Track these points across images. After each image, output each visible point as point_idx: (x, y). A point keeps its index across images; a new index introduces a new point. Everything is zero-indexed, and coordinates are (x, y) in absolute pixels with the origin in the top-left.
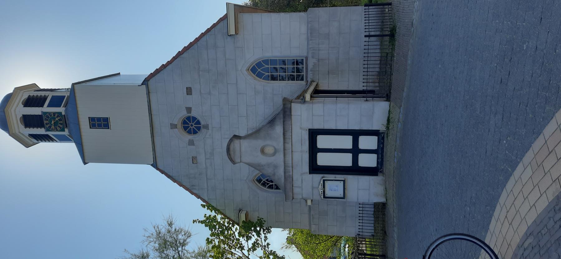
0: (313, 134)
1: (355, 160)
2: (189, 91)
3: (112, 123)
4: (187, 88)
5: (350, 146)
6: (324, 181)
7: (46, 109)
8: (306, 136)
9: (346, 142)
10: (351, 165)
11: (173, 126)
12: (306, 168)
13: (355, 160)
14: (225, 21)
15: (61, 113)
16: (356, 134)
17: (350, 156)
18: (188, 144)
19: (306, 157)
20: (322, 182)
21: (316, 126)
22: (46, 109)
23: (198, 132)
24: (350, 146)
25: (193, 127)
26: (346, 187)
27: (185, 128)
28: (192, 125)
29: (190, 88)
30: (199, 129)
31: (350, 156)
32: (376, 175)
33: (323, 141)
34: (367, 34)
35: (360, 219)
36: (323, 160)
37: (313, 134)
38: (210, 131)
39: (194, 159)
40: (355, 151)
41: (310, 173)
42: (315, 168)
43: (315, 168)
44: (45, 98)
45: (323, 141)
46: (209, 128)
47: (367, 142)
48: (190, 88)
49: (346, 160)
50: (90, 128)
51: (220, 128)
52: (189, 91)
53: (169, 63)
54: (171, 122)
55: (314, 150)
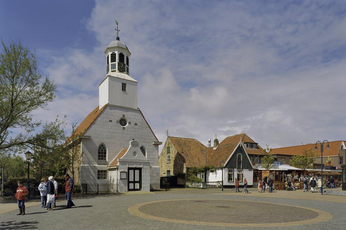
0: (140, 169)
2: (136, 124)
5: (136, 180)
6: (126, 172)
7: (126, 65)
9: (137, 179)
11: (124, 116)
12: (130, 166)
16: (140, 182)
17: (133, 180)
22: (126, 65)
24: (136, 180)
27: (122, 119)
31: (133, 180)
32: (128, 189)
33: (137, 172)
36: (131, 172)
37: (140, 169)
38: (122, 129)
39: (111, 121)
40: (134, 182)
41: (128, 168)
42: (129, 169)
43: (129, 169)
44: (128, 65)
49: (131, 179)
52: (136, 124)
53: (145, 119)
55: (134, 169)
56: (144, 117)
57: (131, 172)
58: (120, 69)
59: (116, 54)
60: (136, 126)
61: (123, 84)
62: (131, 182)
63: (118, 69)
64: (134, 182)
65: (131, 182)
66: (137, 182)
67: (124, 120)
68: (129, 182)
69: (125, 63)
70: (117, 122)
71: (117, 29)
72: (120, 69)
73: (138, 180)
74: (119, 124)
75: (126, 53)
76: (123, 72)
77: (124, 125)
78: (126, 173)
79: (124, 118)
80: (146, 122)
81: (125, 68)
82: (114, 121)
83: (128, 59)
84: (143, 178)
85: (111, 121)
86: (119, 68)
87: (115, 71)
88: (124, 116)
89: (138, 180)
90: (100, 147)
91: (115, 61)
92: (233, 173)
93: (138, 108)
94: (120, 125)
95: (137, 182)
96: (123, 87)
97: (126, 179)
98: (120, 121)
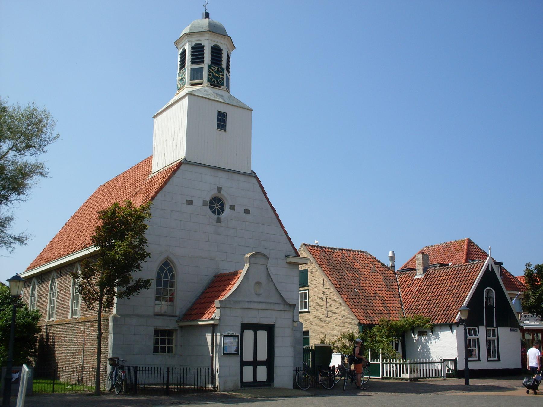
0: (270, 329)
2: (247, 212)
4: (250, 210)
5: (259, 359)
6: (238, 336)
9: (262, 356)
11: (219, 189)
12: (246, 321)
14: (294, 254)
16: (270, 363)
17: (251, 359)
18: (204, 199)
19: (255, 321)
20: (237, 334)
23: (211, 211)
24: (259, 359)
25: (216, 207)
26: (231, 355)
27: (214, 199)
28: (217, 206)
29: (250, 213)
30: (214, 212)
31: (251, 359)
33: (262, 335)
34: (170, 369)
35: (146, 368)
37: (270, 329)
38: (215, 223)
39: (189, 202)
40: (255, 363)
42: (245, 327)
46: (217, 223)
47: (262, 372)
48: (250, 213)
49: (248, 356)
50: (226, 113)
51: (218, 234)
52: (247, 212)
53: (268, 199)
54: (223, 188)
55: (255, 328)
56: (265, 194)
57: (249, 335)
58: (213, 80)
59: (203, 47)
60: (248, 217)
61: (219, 113)
62: (248, 363)
63: (209, 80)
64: (255, 363)
65: (248, 363)
66: (262, 363)
67: (220, 200)
68: (243, 363)
69: (224, 66)
70: (205, 203)
72: (213, 80)
74: (208, 207)
75: (226, 45)
76: (219, 87)
77: (219, 213)
78: (237, 338)
79: (219, 195)
80: (271, 205)
81: (223, 79)
82: (197, 203)
83: (228, 58)
84: (278, 351)
85: (189, 202)
86: (210, 77)
87: (201, 84)
88: (219, 189)
90: (161, 269)
91: (202, 62)
92: (496, 337)
94: (210, 212)
95: (262, 363)
96: (219, 120)
97: (238, 354)
98: (211, 202)
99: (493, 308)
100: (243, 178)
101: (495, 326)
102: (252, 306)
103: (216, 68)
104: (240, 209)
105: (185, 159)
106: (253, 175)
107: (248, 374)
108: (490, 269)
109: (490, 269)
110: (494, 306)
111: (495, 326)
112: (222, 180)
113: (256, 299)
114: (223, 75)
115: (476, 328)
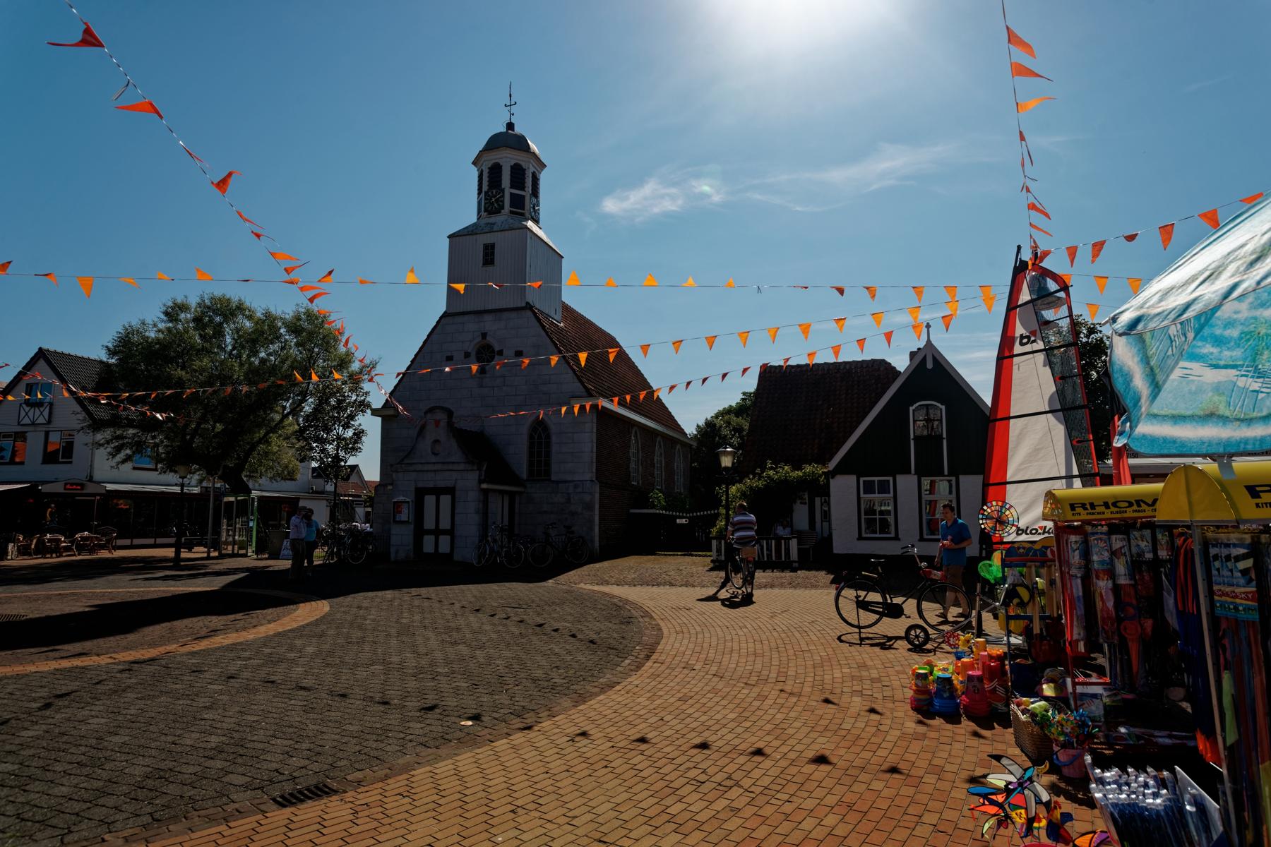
1: (429, 532)
3: (490, 268)
8: (449, 484)
9: (445, 524)
10: (425, 528)
11: (484, 335)
12: (420, 485)
13: (429, 532)
14: (585, 394)
15: (503, 209)
16: (451, 532)
17: (433, 527)
19: (431, 485)
21: (458, 494)
31: (433, 527)
33: (445, 500)
36: (430, 500)
37: (450, 491)
40: (437, 532)
43: (420, 493)
45: (445, 500)
47: (444, 542)
49: (429, 523)
55: (438, 492)
64: (437, 532)
71: (508, 104)
73: (449, 527)
76: (500, 212)
89: (449, 527)
93: (528, 303)
99: (941, 437)
100: (514, 315)
101: (946, 473)
102: (426, 467)
103: (494, 191)
104: (509, 352)
105: (445, 312)
106: (529, 307)
107: (428, 544)
108: (930, 365)
109: (930, 365)
110: (945, 436)
111: (946, 473)
112: (489, 324)
113: (433, 459)
114: (503, 196)
115: (891, 479)
